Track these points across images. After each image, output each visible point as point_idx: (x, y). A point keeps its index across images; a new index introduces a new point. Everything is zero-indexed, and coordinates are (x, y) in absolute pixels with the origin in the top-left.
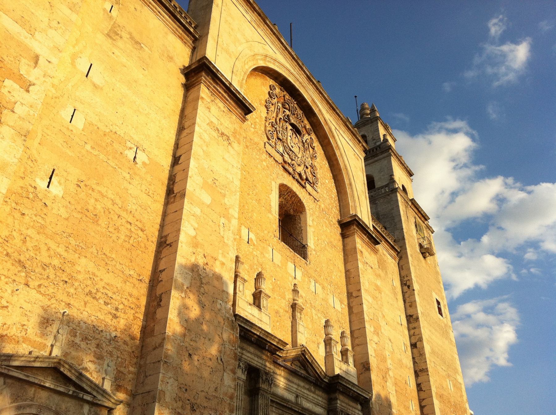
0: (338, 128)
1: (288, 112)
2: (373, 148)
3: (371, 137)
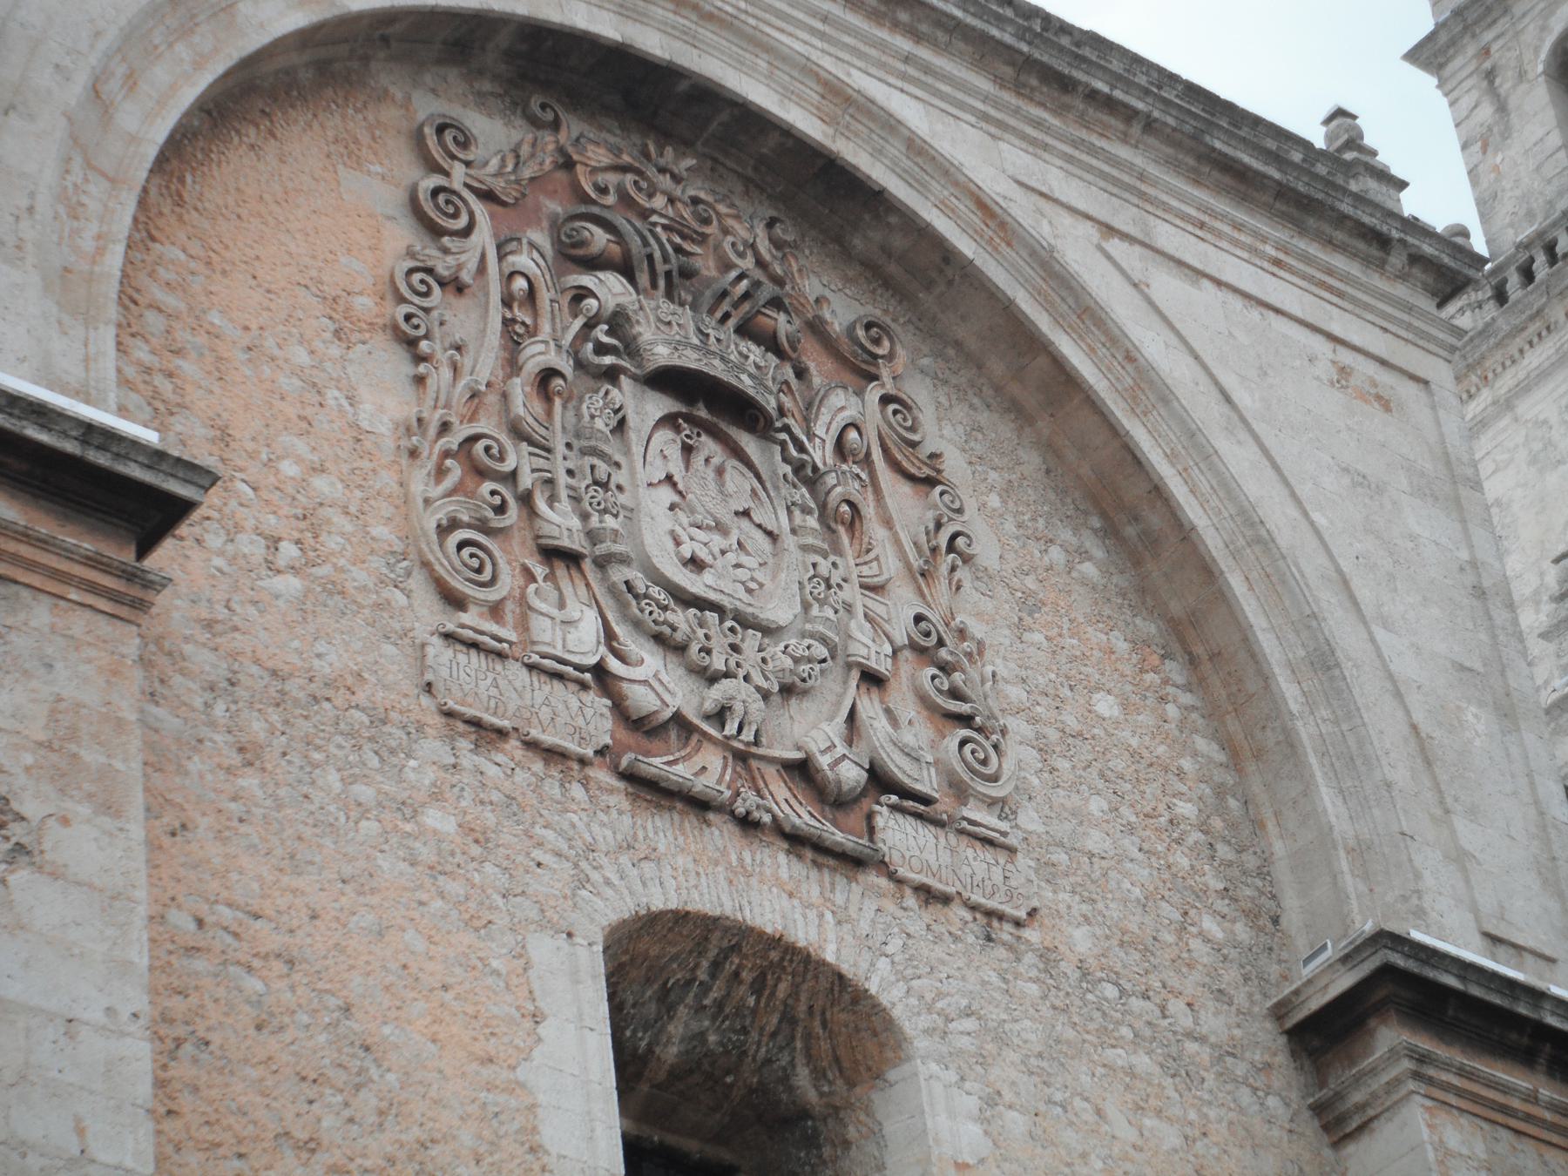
0: (1125, 217)
1: (610, 289)
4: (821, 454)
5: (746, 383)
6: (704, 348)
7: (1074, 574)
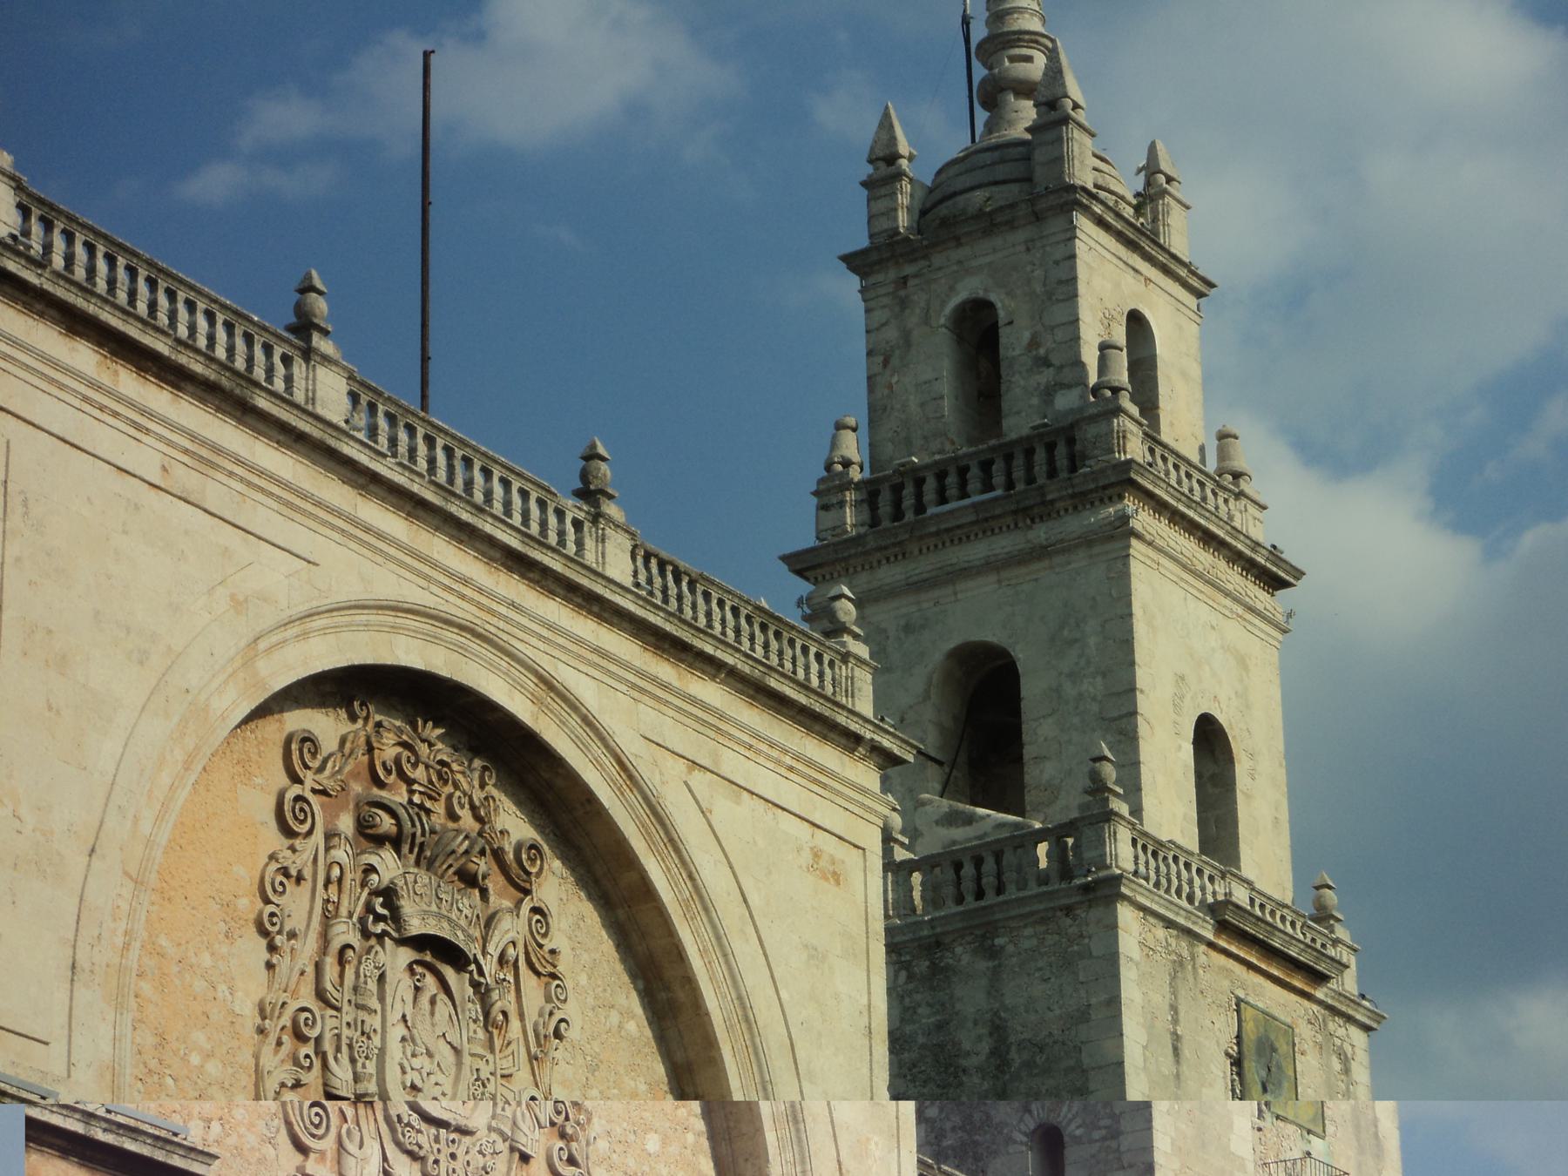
1: (388, 865)
2: (1028, 438)
3: (1027, 335)
4: (490, 966)
5: (460, 940)
6: (440, 916)
7: (623, 1033)
